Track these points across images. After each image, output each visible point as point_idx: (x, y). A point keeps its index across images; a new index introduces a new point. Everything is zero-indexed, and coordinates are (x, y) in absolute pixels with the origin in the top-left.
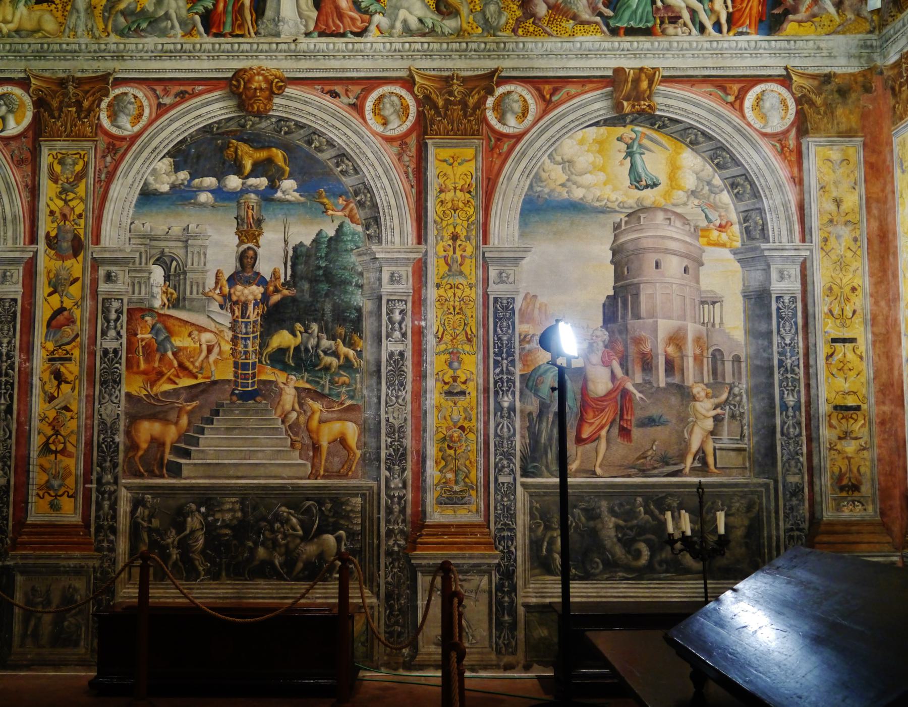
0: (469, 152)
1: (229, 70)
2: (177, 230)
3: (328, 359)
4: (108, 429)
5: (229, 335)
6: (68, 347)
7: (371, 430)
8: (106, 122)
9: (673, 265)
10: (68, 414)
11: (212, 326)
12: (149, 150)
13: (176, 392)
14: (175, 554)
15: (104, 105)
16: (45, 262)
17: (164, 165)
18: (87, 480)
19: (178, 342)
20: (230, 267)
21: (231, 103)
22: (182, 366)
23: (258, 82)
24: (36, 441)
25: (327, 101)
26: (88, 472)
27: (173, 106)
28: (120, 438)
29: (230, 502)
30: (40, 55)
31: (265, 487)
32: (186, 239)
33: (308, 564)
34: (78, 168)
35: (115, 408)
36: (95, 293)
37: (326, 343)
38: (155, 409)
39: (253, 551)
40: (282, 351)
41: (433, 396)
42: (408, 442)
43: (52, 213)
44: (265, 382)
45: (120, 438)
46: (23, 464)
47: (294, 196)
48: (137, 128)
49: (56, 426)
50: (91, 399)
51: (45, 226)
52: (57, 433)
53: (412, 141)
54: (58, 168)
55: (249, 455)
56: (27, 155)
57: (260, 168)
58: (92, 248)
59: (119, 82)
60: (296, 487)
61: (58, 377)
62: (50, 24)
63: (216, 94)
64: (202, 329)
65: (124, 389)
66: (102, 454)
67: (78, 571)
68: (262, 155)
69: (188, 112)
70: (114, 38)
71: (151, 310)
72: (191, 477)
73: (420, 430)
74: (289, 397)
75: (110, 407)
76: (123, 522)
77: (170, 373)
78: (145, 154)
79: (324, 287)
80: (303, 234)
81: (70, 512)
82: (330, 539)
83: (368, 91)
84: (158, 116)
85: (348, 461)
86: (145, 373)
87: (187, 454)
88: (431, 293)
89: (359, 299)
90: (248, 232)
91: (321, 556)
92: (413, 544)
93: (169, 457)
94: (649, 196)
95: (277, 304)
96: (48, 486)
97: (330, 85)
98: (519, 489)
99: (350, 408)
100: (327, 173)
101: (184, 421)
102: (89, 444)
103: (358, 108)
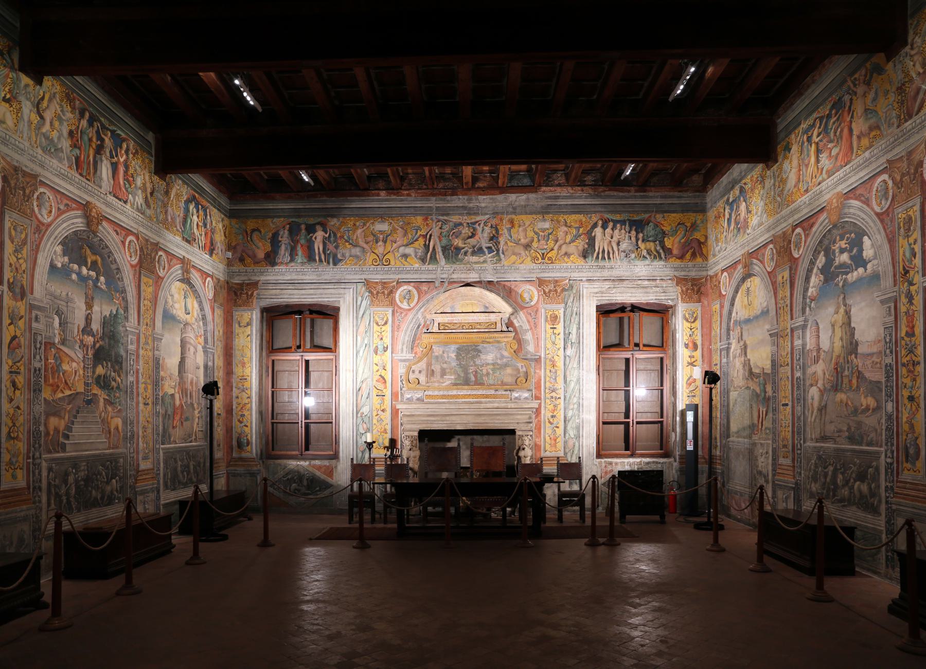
1: (84, 200)
2: (64, 294)
4: (37, 422)
5: (82, 364)
6: (18, 364)
7: (125, 423)
8: (36, 209)
9: (192, 349)
10: (19, 411)
11: (75, 358)
12: (53, 237)
15: (35, 196)
17: (59, 249)
18: (28, 458)
19: (65, 367)
22: (66, 383)
26: (29, 451)
27: (64, 212)
28: (42, 428)
31: (94, 455)
32: (68, 300)
34: (23, 236)
35: (40, 408)
36: (30, 328)
37: (113, 374)
38: (53, 409)
40: (99, 376)
41: (141, 406)
43: (11, 265)
44: (95, 395)
45: (42, 428)
47: (103, 287)
48: (49, 220)
49: (13, 419)
52: (14, 425)
53: (137, 269)
54: (13, 233)
55: (87, 439)
57: (94, 266)
58: (30, 296)
61: (14, 384)
63: (79, 213)
64: (73, 360)
66: (34, 437)
68: (94, 258)
70: (40, 151)
71: (54, 344)
73: (138, 422)
75: (38, 407)
77: (62, 386)
78: (52, 239)
79: (112, 342)
83: (127, 236)
84: (58, 216)
85: (119, 440)
86: (52, 385)
88: (141, 352)
96: (10, 463)
99: (120, 411)
101: (67, 417)
102: (29, 432)
103: (123, 243)
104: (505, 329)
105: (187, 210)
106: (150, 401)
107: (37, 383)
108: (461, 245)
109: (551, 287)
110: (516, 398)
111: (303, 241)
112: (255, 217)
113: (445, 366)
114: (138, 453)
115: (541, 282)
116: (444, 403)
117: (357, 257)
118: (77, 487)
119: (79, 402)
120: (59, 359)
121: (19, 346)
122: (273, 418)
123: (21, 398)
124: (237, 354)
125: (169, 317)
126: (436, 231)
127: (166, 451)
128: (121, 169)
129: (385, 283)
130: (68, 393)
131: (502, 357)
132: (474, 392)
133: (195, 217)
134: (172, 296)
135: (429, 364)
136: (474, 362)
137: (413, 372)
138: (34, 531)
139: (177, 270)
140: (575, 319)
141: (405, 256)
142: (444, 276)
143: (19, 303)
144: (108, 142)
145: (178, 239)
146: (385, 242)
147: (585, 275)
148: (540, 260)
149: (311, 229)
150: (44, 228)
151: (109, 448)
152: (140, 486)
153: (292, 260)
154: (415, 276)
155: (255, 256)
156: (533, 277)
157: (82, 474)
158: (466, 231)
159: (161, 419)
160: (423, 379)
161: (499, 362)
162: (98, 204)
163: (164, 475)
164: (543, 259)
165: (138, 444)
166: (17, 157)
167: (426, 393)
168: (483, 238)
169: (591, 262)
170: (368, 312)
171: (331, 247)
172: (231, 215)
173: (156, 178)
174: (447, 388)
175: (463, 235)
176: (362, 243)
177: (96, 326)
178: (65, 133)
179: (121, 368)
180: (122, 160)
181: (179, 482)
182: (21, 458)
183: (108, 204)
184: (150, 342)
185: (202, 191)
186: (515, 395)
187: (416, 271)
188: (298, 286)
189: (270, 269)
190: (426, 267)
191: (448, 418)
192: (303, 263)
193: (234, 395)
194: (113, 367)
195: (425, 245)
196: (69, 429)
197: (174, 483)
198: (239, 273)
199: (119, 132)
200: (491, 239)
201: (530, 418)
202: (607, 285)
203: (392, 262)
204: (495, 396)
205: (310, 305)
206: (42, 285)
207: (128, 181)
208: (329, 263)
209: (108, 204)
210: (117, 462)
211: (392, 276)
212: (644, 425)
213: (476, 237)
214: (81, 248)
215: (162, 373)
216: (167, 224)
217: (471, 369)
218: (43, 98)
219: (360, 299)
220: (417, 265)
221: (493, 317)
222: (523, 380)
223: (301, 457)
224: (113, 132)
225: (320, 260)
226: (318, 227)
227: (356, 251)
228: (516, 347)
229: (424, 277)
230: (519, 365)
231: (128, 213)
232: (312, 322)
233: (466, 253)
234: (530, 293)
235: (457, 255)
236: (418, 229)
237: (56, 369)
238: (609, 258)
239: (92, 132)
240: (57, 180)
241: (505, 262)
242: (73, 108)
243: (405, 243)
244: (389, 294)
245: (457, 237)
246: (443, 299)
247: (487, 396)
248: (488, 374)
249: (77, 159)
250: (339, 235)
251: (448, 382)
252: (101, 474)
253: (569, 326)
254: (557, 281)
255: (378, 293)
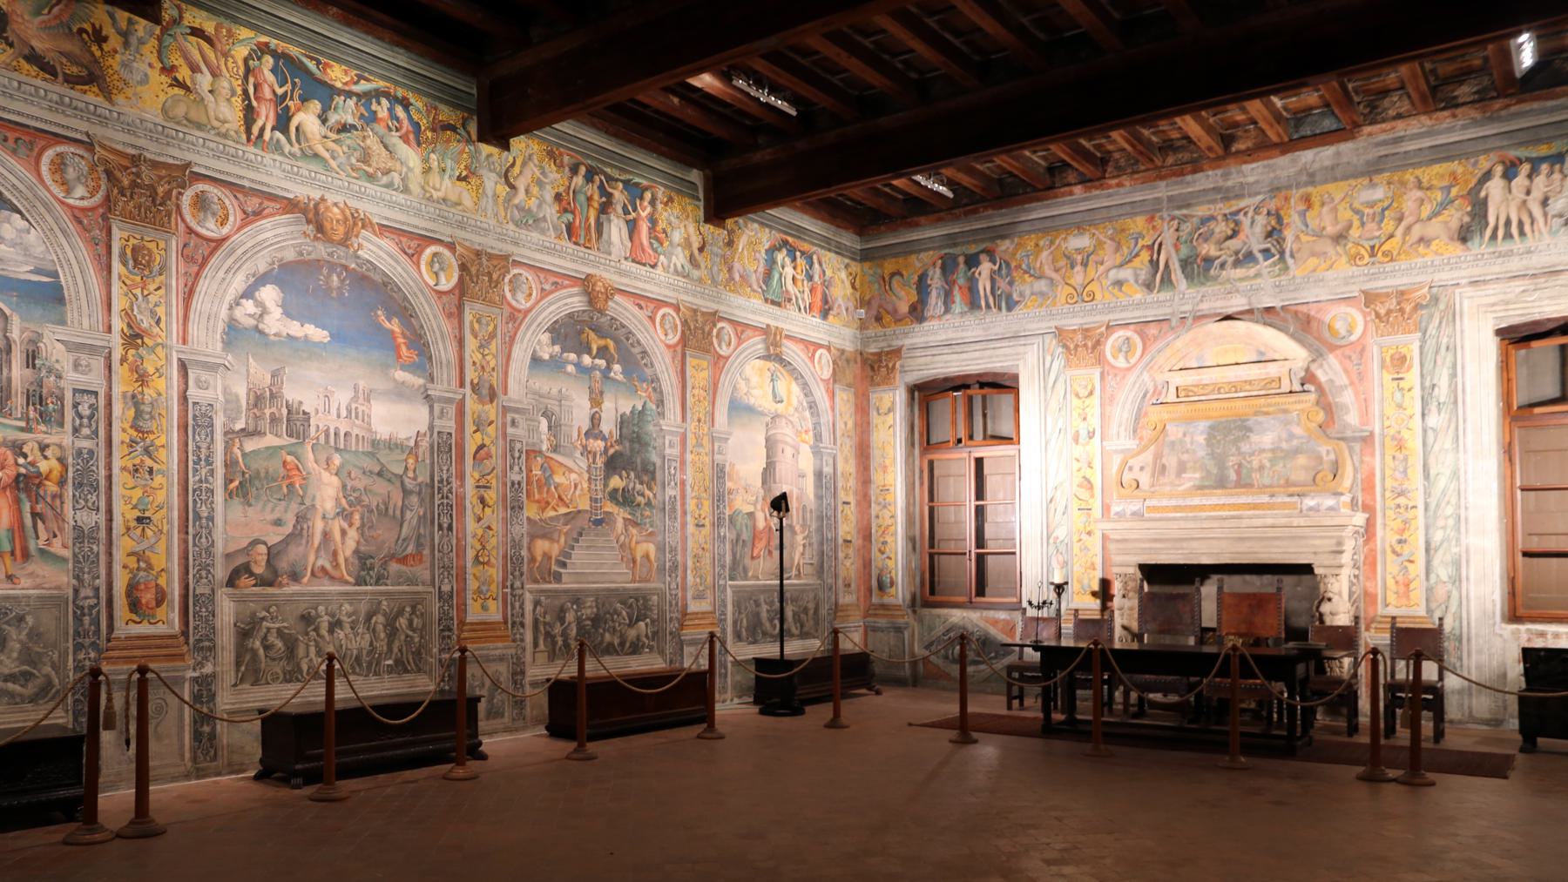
0: (705, 364)
2: (555, 391)
3: (639, 499)
4: (516, 545)
5: (586, 476)
7: (661, 549)
8: (508, 295)
9: (789, 451)
11: (575, 468)
13: (557, 517)
14: (560, 641)
16: (471, 405)
17: (545, 338)
18: (504, 587)
19: (558, 479)
20: (586, 426)
21: (585, 299)
23: (599, 287)
24: (470, 554)
25: (635, 310)
26: (505, 579)
27: (551, 292)
28: (524, 553)
29: (590, 601)
30: (461, 225)
31: (608, 590)
33: (632, 643)
34: (491, 328)
35: (520, 530)
36: (505, 435)
37: (638, 487)
38: (540, 531)
39: (603, 636)
40: (615, 490)
41: (691, 528)
42: (679, 558)
44: (607, 513)
45: (524, 553)
46: (462, 571)
47: (620, 377)
50: (505, 520)
51: (471, 374)
52: (484, 548)
53: (679, 349)
54: (476, 326)
55: (597, 567)
56: (454, 310)
57: (603, 352)
58: (502, 397)
59: (516, 263)
60: (625, 589)
61: (482, 500)
62: (468, 202)
63: (576, 290)
65: (526, 513)
66: (513, 564)
67: (501, 659)
68: (602, 342)
69: (560, 299)
70: (511, 226)
71: (540, 452)
72: (568, 584)
73: (685, 550)
74: (620, 524)
76: (528, 620)
79: (636, 446)
80: (626, 407)
81: (494, 613)
82: (642, 624)
83: (658, 308)
85: (650, 570)
87: (564, 565)
88: (689, 457)
89: (654, 457)
90: (596, 401)
91: (638, 638)
92: (682, 626)
93: (554, 568)
94: (780, 407)
95: (613, 456)
96: (479, 591)
97: (640, 299)
98: (729, 591)
99: (651, 534)
100: (637, 364)
101: (562, 540)
102: (505, 557)
103: (652, 319)
104: (1297, 387)
105: (771, 263)
106: (707, 522)
107: (516, 499)
108: (1213, 252)
109: (1392, 304)
110: (1311, 509)
111: (961, 281)
112: (895, 256)
113: (1185, 457)
114: (684, 589)
115: (1370, 298)
116: (1174, 519)
117: (1042, 294)
118: (580, 627)
119: (582, 522)
120: (549, 468)
121: (489, 456)
122: (932, 546)
123: (493, 517)
124: (875, 454)
125: (740, 409)
126: (1168, 237)
127: (737, 591)
128: (644, 227)
129: (1087, 330)
130: (563, 510)
131: (1291, 436)
132: (1232, 500)
133: (789, 271)
134: (747, 380)
135: (1158, 456)
136: (1238, 449)
137: (1131, 469)
138: (514, 674)
139: (756, 344)
140: (1445, 359)
141: (1119, 283)
142: (1187, 308)
143: (488, 407)
144: (619, 195)
145: (757, 302)
146: (1085, 264)
147: (1463, 274)
148: (1367, 259)
149: (972, 262)
150: (520, 316)
151: (633, 581)
152: (688, 634)
153: (947, 311)
154: (1137, 313)
155: (896, 311)
156: (1354, 290)
157: (588, 612)
158: (1221, 228)
159: (728, 546)
160: (1145, 479)
161: (1284, 445)
162: (605, 275)
163: (735, 623)
164: (1373, 255)
165: (685, 578)
166: (477, 239)
167: (1148, 503)
168: (1253, 235)
169: (1478, 246)
170: (1061, 379)
171: (1002, 284)
172: (865, 256)
173: (708, 229)
174: (1185, 494)
175: (1217, 236)
176: (1049, 272)
177: (608, 426)
178: (549, 195)
179: (654, 479)
180: (644, 214)
181: (765, 634)
182: (493, 587)
183: (622, 273)
184: (706, 441)
185: (800, 232)
186: (1309, 502)
187: (1138, 305)
188: (957, 348)
189: (917, 327)
190: (1154, 296)
191: (1185, 545)
192: (962, 314)
193: (873, 514)
194: (637, 477)
195: (1151, 261)
196: (569, 556)
197: (753, 632)
198: (876, 338)
199: (637, 180)
200: (1269, 235)
201: (1340, 543)
202: (1517, 286)
203: (1098, 296)
204: (1270, 506)
205: (979, 375)
206: (519, 382)
207: (657, 239)
208: (1000, 309)
209: (622, 273)
210: (646, 600)
211: (1098, 318)
212: (1554, 560)
213: (1242, 236)
214: (581, 332)
215: (729, 484)
216: (733, 283)
217: (1232, 461)
218: (513, 165)
219: (1049, 359)
220: (1138, 296)
221: (1272, 370)
222: (1326, 476)
223: (970, 605)
224: (626, 183)
225: (988, 306)
226: (983, 257)
227: (1041, 285)
228: (1321, 416)
229: (1150, 314)
230: (1323, 450)
231: (665, 278)
232: (984, 398)
233: (1222, 266)
234: (1349, 320)
235: (1207, 270)
236: (1141, 236)
237: (544, 483)
238: (1522, 233)
239: (593, 190)
240: (538, 256)
241: (1296, 270)
242: (560, 166)
243: (1118, 262)
244: (1094, 347)
245: (1206, 240)
246: (1183, 345)
247: (1255, 507)
248: (1261, 468)
249: (570, 229)
250: (1013, 264)
251: (1189, 484)
252: (619, 615)
253: (1432, 373)
254: (1402, 293)
255: (1077, 346)
